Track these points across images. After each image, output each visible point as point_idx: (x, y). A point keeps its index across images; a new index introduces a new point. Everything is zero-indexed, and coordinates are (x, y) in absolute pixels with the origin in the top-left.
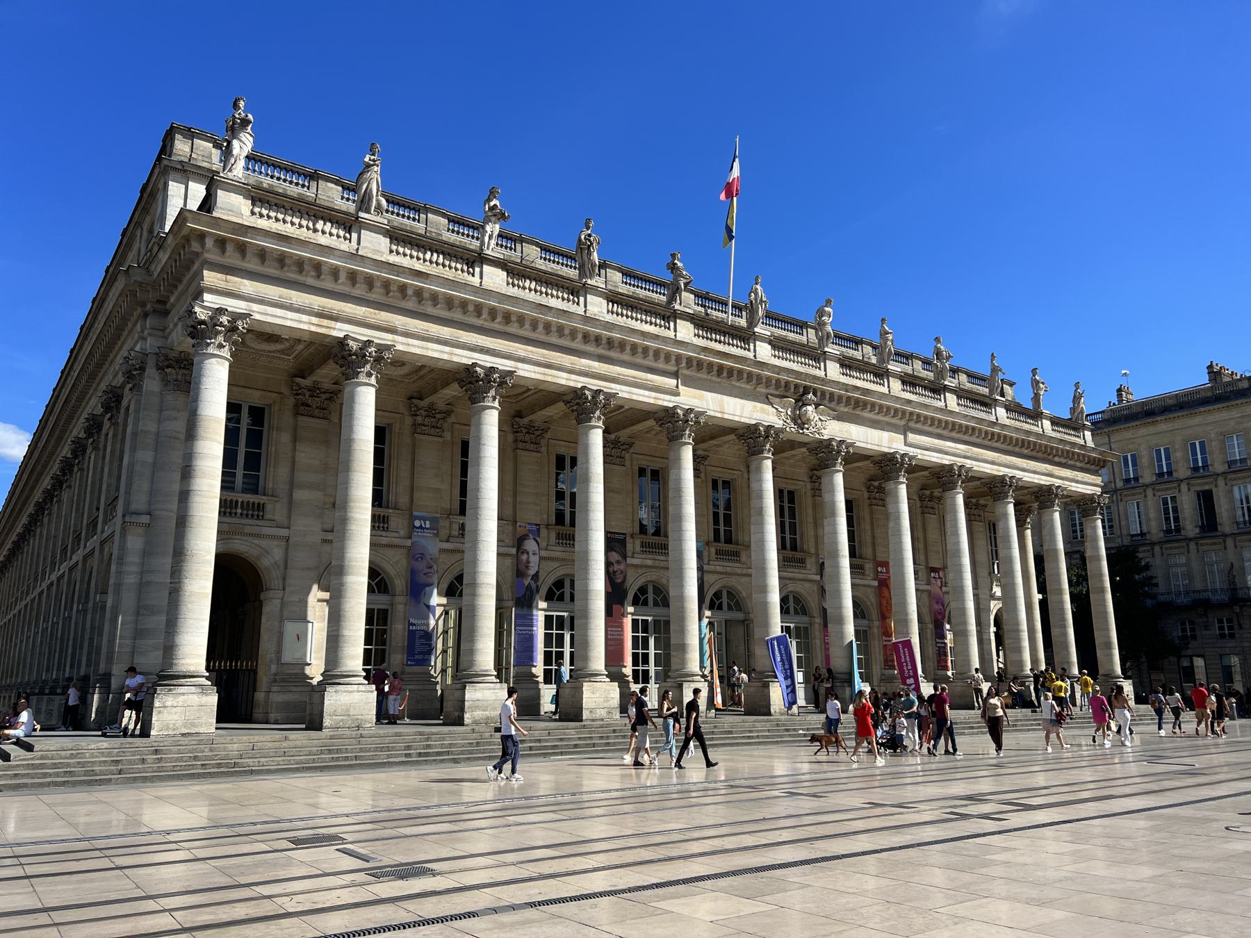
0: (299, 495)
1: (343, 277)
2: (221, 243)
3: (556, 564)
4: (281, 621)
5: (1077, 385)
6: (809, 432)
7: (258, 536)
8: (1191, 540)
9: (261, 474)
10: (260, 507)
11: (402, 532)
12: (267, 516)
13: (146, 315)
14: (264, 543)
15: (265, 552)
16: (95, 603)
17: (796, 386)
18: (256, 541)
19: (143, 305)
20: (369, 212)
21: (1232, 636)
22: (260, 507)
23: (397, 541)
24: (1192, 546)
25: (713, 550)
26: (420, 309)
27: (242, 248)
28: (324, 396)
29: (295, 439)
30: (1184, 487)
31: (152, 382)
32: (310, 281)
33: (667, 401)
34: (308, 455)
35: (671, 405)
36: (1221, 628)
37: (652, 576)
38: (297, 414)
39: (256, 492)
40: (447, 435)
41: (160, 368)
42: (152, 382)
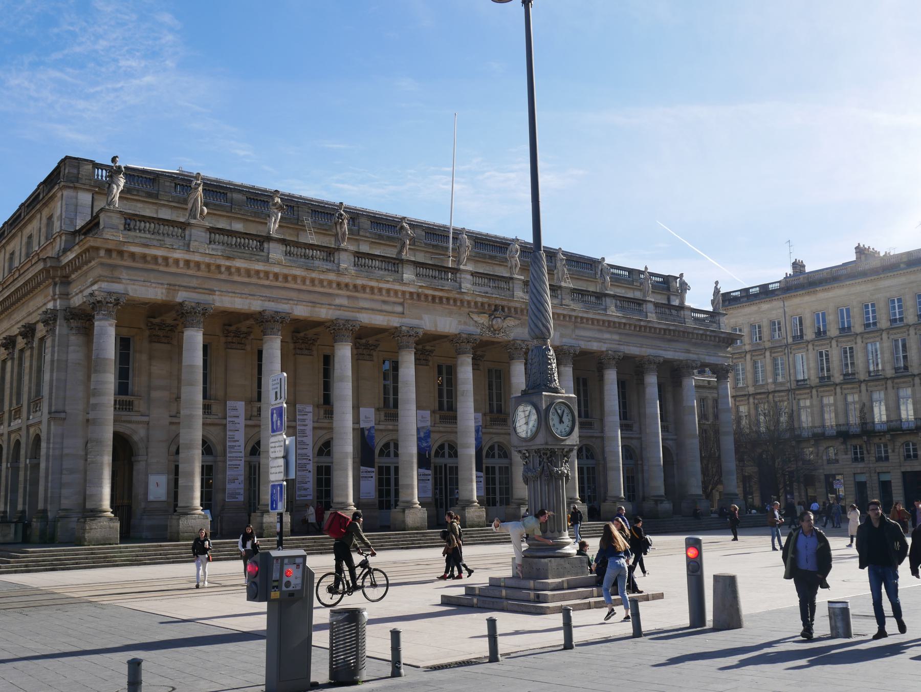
0: (155, 394)
1: (181, 264)
2: (109, 251)
3: (324, 432)
4: (147, 475)
5: (717, 283)
6: (501, 337)
7: (130, 422)
8: (837, 385)
9: (130, 382)
10: (130, 403)
11: (220, 415)
12: (135, 409)
13: (55, 284)
14: (133, 426)
15: (138, 433)
16: (26, 465)
17: (489, 305)
18: (129, 425)
19: (53, 278)
20: (195, 218)
21: (862, 459)
22: (130, 403)
23: (217, 421)
24: (838, 390)
25: (438, 416)
26: (230, 278)
27: (121, 253)
28: (167, 329)
29: (151, 358)
30: (834, 343)
31: (60, 328)
32: (162, 268)
33: (395, 322)
34: (159, 369)
35: (398, 325)
36: (856, 453)
37: (394, 437)
38: (151, 342)
39: (127, 394)
40: (248, 348)
41: (67, 319)
42: (60, 328)
